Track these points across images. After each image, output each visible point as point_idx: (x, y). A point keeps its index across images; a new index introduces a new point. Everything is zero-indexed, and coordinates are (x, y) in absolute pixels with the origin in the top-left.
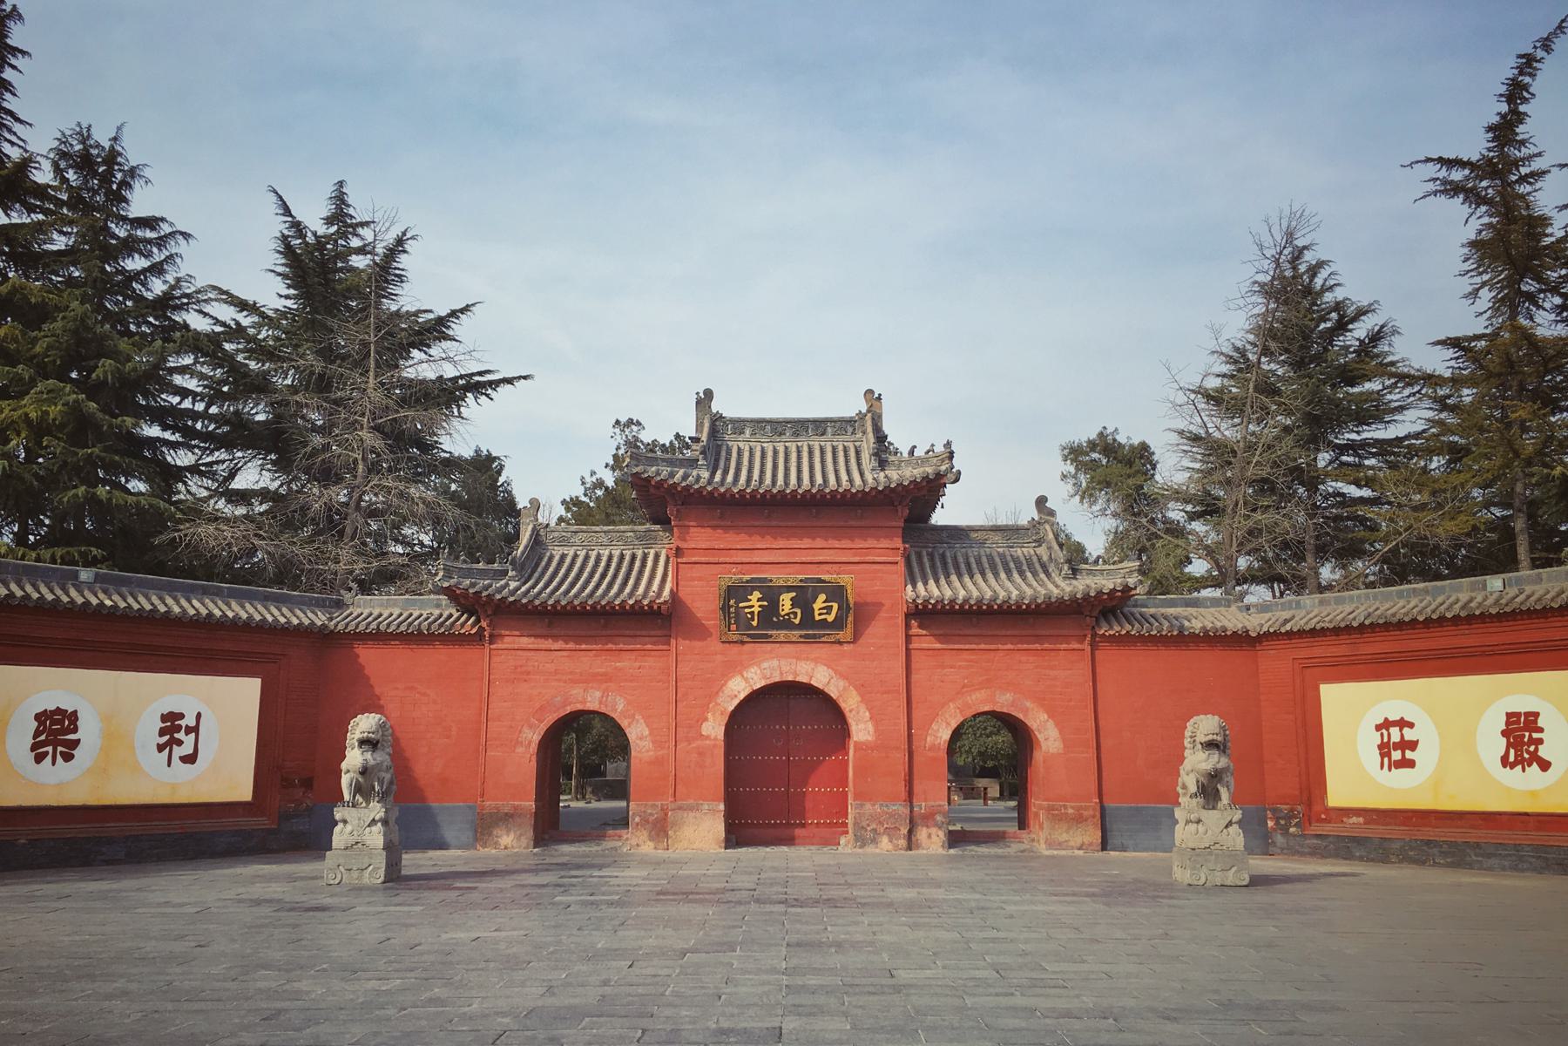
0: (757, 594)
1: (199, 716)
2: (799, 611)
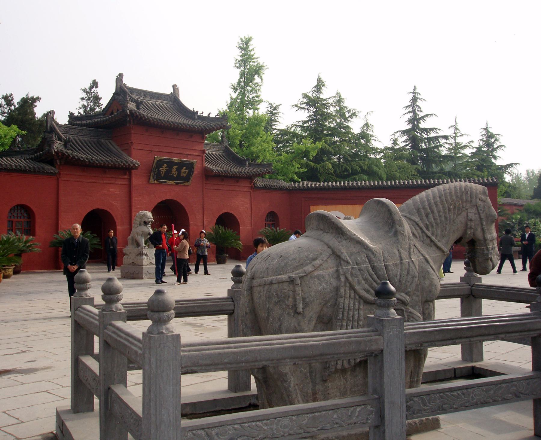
0: (165, 165)
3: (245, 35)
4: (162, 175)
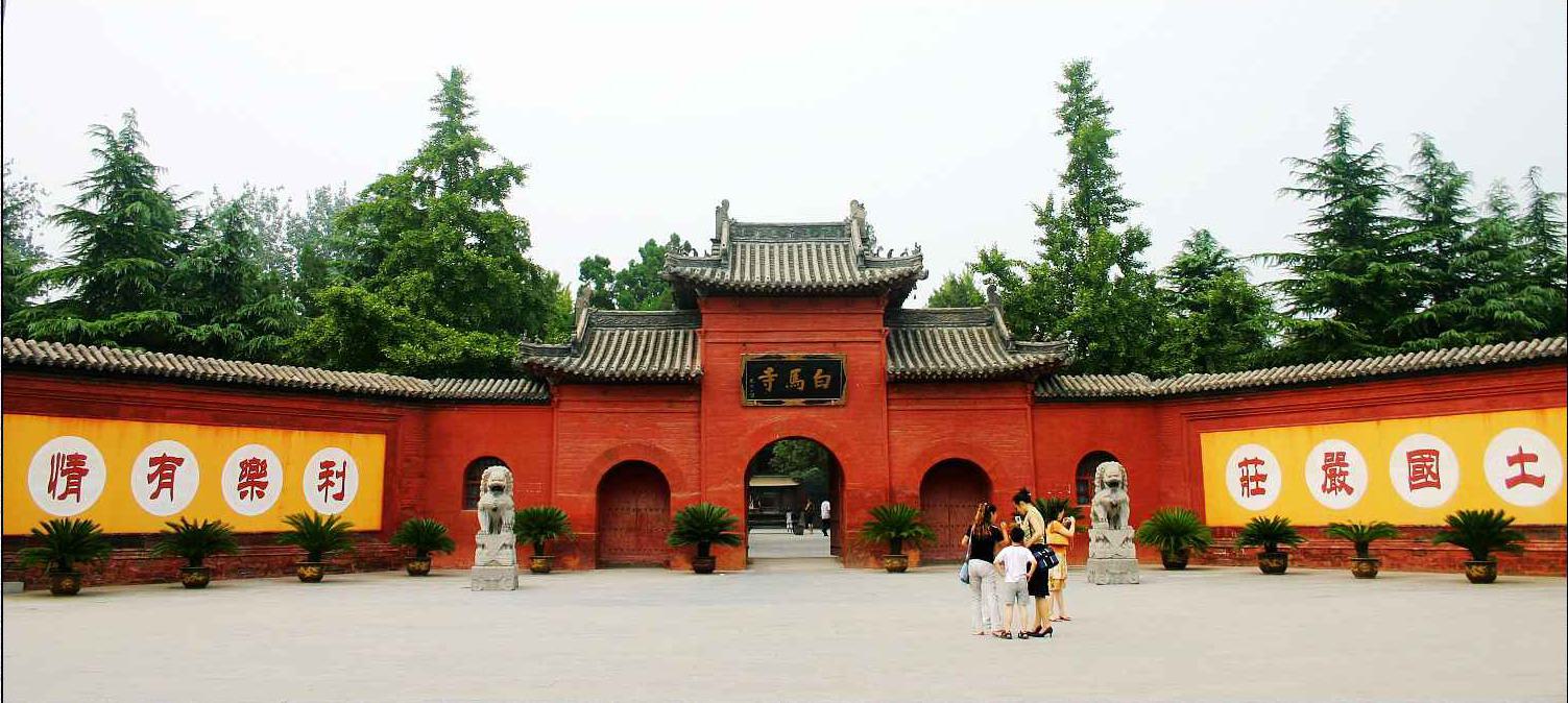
1: (345, 463)
2: (803, 382)
3: (1079, 57)
4: (769, 389)
